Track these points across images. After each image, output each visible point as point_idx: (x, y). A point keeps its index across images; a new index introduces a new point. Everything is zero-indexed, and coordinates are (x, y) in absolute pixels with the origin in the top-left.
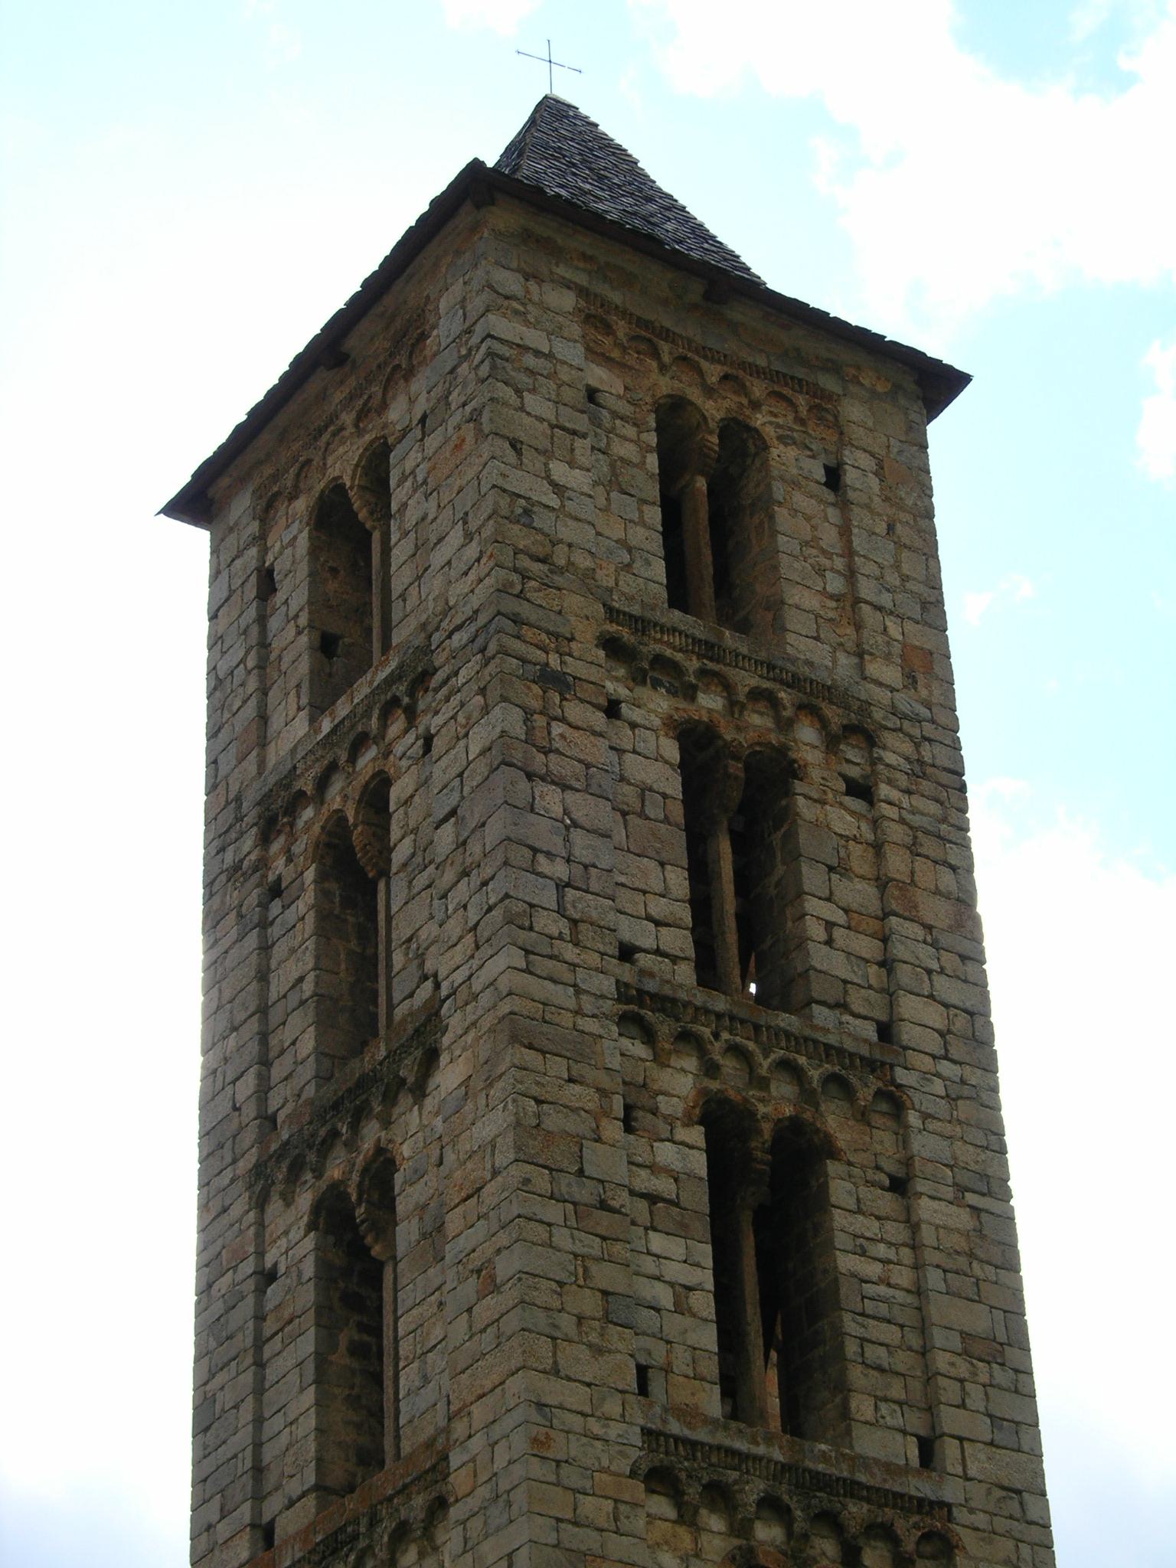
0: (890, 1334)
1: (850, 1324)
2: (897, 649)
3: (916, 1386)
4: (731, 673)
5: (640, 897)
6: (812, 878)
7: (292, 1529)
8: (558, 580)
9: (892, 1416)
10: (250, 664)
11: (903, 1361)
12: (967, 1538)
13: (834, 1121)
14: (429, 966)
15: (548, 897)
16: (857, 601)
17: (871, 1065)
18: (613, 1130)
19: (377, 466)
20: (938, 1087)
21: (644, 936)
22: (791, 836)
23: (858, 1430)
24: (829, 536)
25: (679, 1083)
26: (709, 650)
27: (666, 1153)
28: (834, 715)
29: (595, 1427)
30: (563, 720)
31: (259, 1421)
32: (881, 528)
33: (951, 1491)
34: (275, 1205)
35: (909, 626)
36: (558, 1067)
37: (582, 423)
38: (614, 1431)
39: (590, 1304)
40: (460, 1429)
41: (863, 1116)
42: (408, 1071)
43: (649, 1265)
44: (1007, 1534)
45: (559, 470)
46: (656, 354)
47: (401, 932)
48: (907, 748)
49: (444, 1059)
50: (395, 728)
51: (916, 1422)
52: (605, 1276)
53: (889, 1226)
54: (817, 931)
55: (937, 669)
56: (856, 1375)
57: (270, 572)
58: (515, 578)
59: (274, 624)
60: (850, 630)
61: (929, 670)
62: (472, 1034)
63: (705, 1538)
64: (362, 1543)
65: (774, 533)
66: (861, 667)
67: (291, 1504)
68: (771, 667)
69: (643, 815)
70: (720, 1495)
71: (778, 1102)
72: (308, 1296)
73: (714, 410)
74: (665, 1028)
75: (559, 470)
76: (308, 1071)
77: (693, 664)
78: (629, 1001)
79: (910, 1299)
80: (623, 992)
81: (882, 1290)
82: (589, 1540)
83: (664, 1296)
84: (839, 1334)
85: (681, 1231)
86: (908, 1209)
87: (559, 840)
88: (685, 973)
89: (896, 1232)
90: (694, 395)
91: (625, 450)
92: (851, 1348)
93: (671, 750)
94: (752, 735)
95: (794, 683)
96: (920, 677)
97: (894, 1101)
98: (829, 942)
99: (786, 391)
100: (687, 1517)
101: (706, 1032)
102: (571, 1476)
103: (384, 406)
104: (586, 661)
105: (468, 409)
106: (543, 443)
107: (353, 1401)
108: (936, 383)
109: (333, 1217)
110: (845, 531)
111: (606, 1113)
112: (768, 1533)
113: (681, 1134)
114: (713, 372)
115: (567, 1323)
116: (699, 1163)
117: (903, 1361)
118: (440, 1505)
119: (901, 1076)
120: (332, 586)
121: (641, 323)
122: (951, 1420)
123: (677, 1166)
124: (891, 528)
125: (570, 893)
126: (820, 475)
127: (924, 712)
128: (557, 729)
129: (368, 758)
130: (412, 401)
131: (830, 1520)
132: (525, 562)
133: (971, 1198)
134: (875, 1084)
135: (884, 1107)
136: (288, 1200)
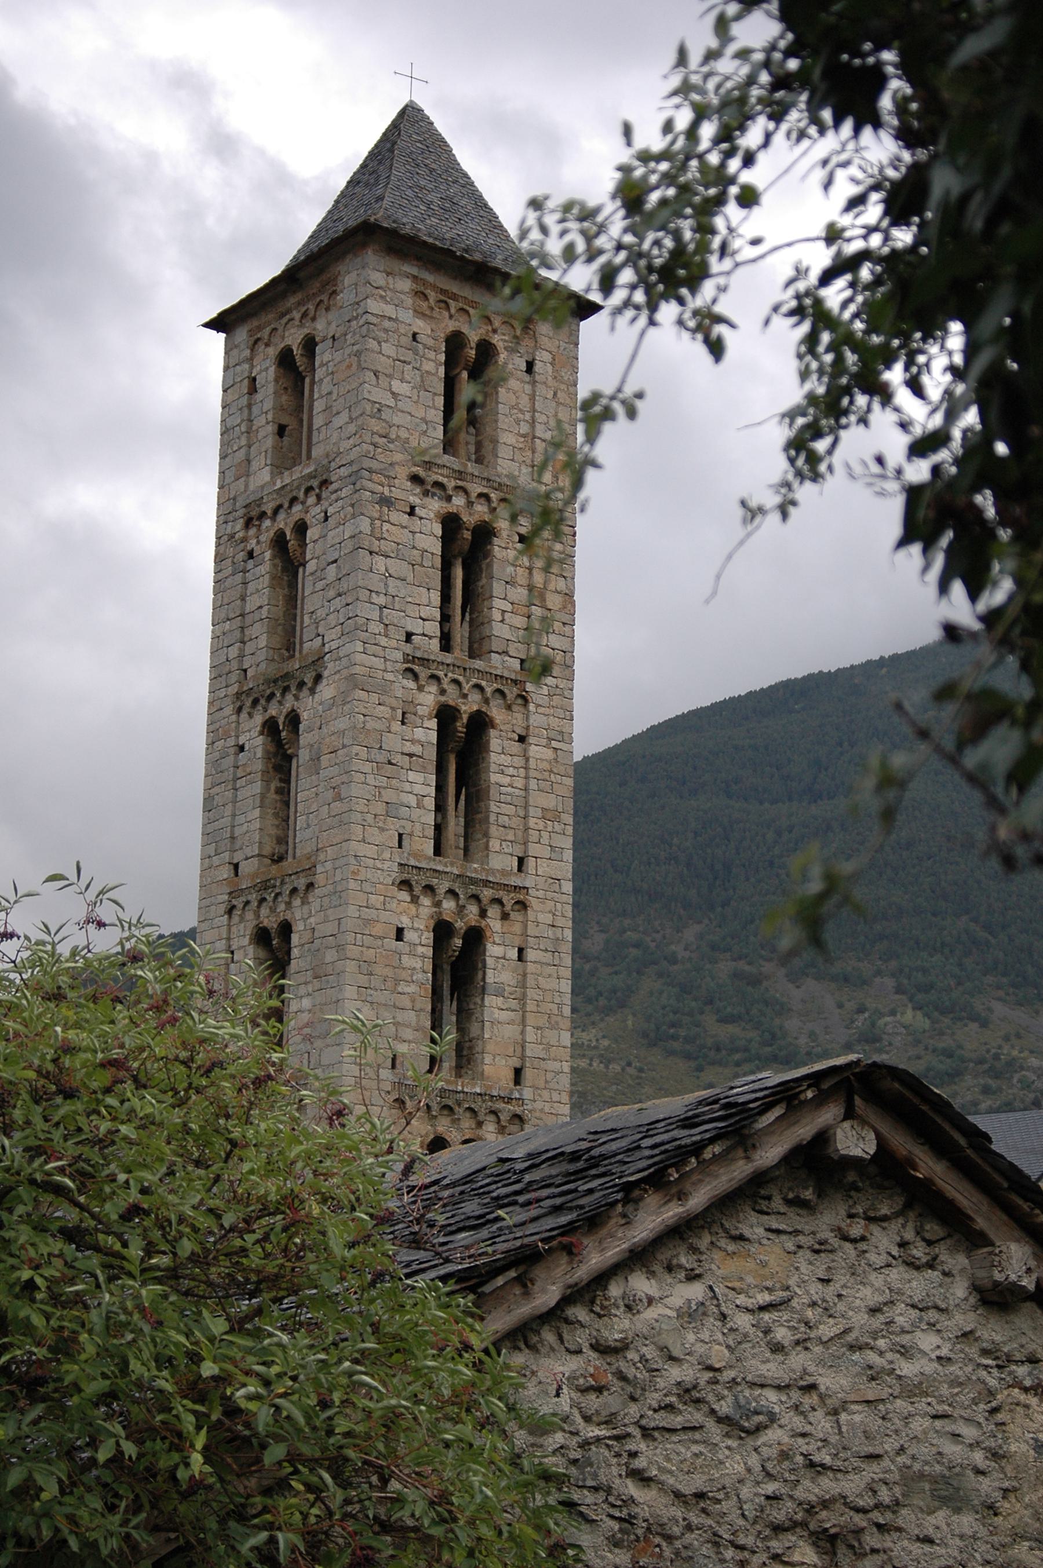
0: (510, 810)
1: (493, 807)
3: (520, 833)
4: (469, 486)
5: (417, 608)
6: (498, 588)
7: (247, 870)
10: (243, 429)
11: (516, 822)
12: (533, 902)
13: (496, 712)
14: (321, 630)
15: (376, 615)
16: (534, 437)
17: (515, 682)
18: (396, 726)
19: (310, 345)
21: (415, 626)
22: (490, 566)
23: (491, 855)
24: (525, 402)
25: (428, 700)
26: (460, 475)
27: (419, 733)
29: (379, 864)
30: (388, 522)
31: (234, 815)
32: (550, 395)
34: (244, 715)
36: (374, 698)
37: (409, 356)
38: (387, 864)
39: (380, 808)
40: (322, 857)
41: (509, 708)
42: (308, 679)
43: (407, 787)
44: (552, 900)
45: (397, 386)
46: (448, 308)
47: (309, 607)
49: (324, 682)
50: (312, 500)
51: (519, 851)
52: (389, 795)
53: (516, 759)
54: (497, 615)
56: (493, 830)
57: (254, 379)
58: (371, 448)
59: (255, 410)
60: (529, 453)
62: (337, 677)
63: (421, 908)
64: (277, 890)
65: (498, 403)
67: (247, 859)
68: (489, 480)
70: (429, 889)
71: (469, 706)
72: (259, 766)
73: (473, 337)
74: (423, 673)
75: (397, 386)
76: (262, 655)
78: (408, 662)
79: (522, 793)
80: (408, 659)
81: (509, 790)
82: (372, 914)
83: (412, 801)
84: (488, 811)
85: (423, 770)
86: (525, 750)
87: (382, 585)
88: (435, 644)
89: (519, 761)
90: (465, 329)
91: (429, 366)
92: (492, 818)
93: (438, 530)
95: (499, 487)
100: (415, 900)
101: (441, 674)
102: (367, 887)
103: (314, 319)
105: (355, 348)
106: (390, 371)
107: (276, 815)
109: (270, 727)
110: (533, 398)
111: (394, 718)
112: (449, 905)
115: (370, 818)
116: (433, 736)
117: (516, 822)
118: (310, 886)
120: (284, 398)
121: (443, 292)
122: (533, 849)
123: (423, 739)
124: (555, 394)
128: (386, 526)
129: (297, 508)
130: (329, 323)
131: (476, 898)
132: (377, 439)
133: (554, 744)
135: (520, 701)
136: (250, 715)
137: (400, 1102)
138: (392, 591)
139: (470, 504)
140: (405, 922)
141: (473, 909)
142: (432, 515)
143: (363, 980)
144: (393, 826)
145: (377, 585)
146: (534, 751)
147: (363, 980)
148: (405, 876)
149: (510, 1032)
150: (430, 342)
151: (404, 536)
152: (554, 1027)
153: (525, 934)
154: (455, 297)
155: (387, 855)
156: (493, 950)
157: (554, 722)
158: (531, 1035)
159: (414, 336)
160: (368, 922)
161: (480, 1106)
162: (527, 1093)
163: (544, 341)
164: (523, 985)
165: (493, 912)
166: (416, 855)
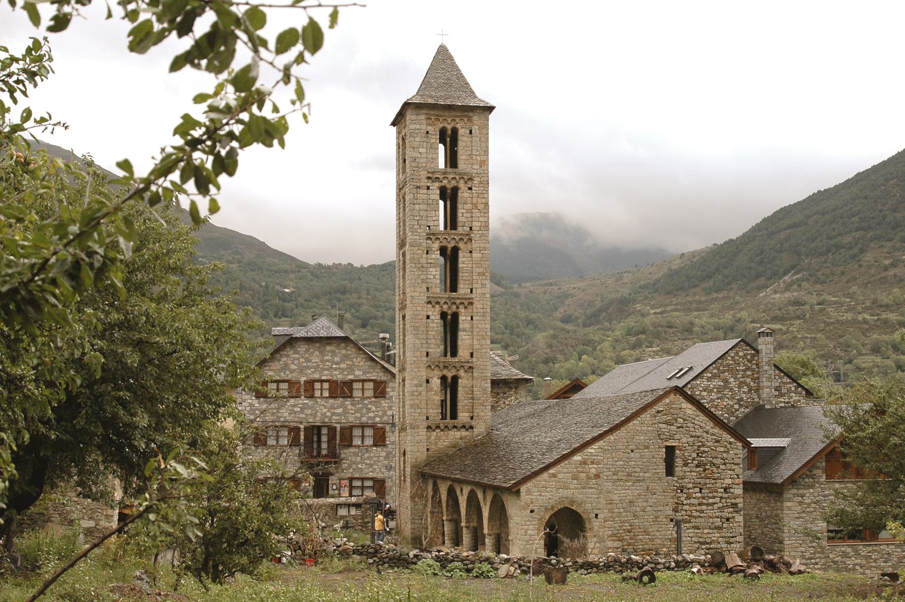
9: (466, 286)
18: (425, 256)
25: (436, 245)
27: (433, 256)
33: (473, 296)
39: (420, 281)
52: (422, 277)
70: (438, 303)
73: (449, 127)
74: (433, 238)
75: (421, 150)
77: (441, 177)
80: (427, 234)
83: (432, 277)
90: (446, 125)
93: (438, 192)
97: (470, 240)
100: (433, 307)
104: (425, 182)
108: (491, 109)
114: (449, 120)
122: (475, 286)
139: (449, 182)
140: (430, 313)
141: (454, 307)
143: (415, 332)
144: (424, 286)
146: (474, 255)
147: (415, 332)
149: (468, 342)
151: (425, 197)
152: (484, 339)
156: (461, 318)
157: (482, 245)
158: (475, 342)
159: (427, 133)
160: (417, 315)
161: (457, 365)
162: (474, 360)
164: (472, 327)
166: (433, 293)
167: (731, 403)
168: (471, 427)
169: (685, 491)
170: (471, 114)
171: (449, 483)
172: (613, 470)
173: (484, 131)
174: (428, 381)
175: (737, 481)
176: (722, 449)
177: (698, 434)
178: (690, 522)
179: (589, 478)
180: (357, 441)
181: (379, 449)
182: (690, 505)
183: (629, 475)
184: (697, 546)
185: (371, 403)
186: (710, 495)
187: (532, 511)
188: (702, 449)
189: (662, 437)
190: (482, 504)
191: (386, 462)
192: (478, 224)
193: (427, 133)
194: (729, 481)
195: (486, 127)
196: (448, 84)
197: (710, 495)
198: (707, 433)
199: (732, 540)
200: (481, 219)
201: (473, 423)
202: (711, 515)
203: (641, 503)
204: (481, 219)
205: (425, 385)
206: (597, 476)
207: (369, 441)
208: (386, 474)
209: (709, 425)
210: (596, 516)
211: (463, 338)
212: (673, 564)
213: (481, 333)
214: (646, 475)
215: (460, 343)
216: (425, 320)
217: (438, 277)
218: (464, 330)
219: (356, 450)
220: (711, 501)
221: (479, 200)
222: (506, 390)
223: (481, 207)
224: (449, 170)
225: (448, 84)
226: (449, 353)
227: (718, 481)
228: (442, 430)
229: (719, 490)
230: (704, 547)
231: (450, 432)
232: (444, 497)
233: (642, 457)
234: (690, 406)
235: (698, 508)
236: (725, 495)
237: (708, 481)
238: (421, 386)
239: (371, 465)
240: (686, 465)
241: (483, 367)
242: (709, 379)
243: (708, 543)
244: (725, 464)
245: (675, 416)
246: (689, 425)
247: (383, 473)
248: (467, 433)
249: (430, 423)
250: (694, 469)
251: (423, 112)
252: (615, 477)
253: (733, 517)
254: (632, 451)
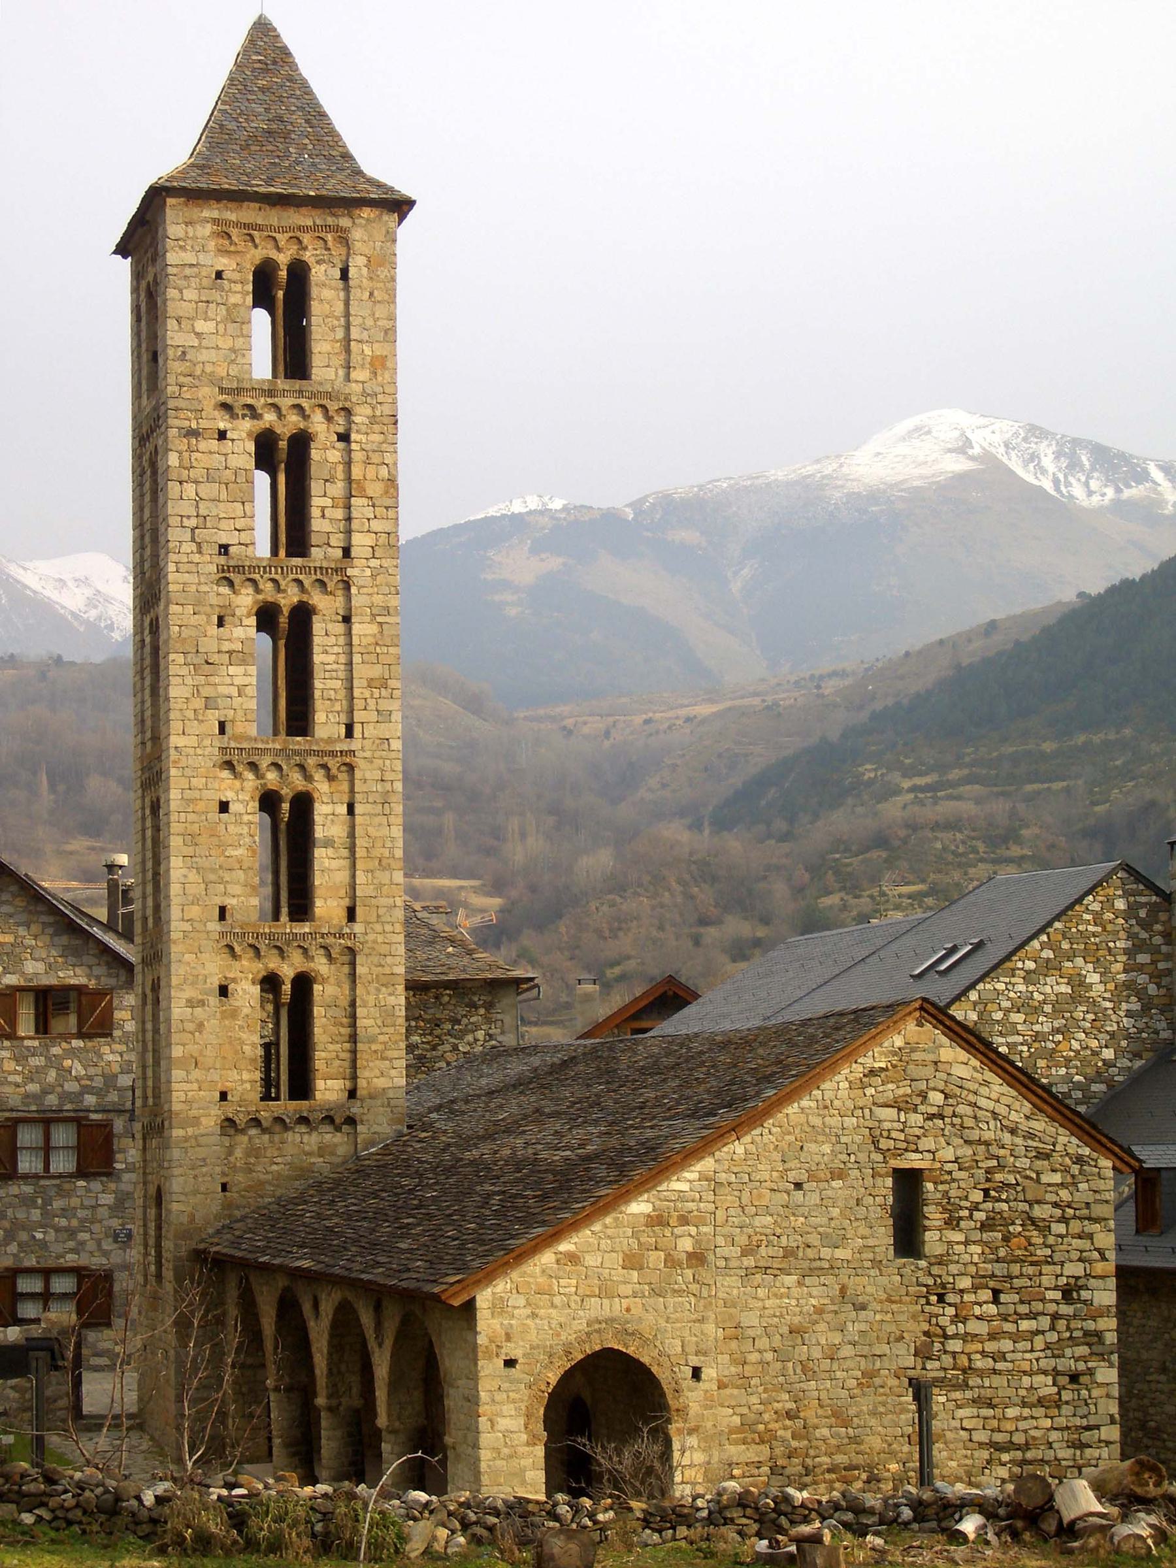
2: (369, 359)
8: (196, 382)
12: (359, 762)
13: (317, 599)
18: (213, 630)
20: (368, 572)
25: (246, 600)
28: (333, 406)
29: (199, 751)
33: (355, 745)
35: (376, 346)
39: (199, 703)
44: (381, 758)
45: (200, 326)
46: (253, 240)
48: (369, 412)
52: (206, 691)
55: (389, 364)
61: (384, 367)
63: (245, 783)
66: (348, 375)
69: (236, 482)
75: (200, 326)
77: (259, 403)
78: (223, 571)
80: (222, 569)
81: (335, 666)
82: (196, 794)
83: (234, 691)
86: (350, 629)
90: (273, 254)
91: (234, 299)
93: (251, 447)
94: (291, 426)
95: (313, 395)
96: (379, 372)
98: (323, 516)
99: (322, 235)
102: (188, 772)
108: (400, 206)
110: (347, 303)
112: (272, 776)
113: (246, 622)
119: (349, 572)
124: (371, 294)
125: (197, 531)
126: (338, 274)
127: (379, 389)
128: (195, 455)
133: (379, 619)
134: (336, 578)
137: (230, 948)
138: (202, 512)
140: (229, 796)
142: (244, 435)
143: (189, 851)
144: (213, 717)
145: (187, 508)
146: (356, 629)
147: (189, 851)
148: (227, 758)
150: (236, 276)
152: (388, 868)
153: (352, 791)
154: (259, 228)
155: (207, 742)
157: (378, 599)
158: (361, 878)
159: (219, 275)
162: (358, 928)
163: (358, 246)
164: (352, 835)
165: (319, 775)
166: (235, 738)
167: (1094, 1044)
168: (351, 1121)
169: (951, 1298)
170: (345, 222)
171: (282, 1282)
172: (742, 1240)
173: (383, 273)
174: (224, 991)
175: (1099, 1268)
176: (1057, 1178)
177: (988, 1135)
178: (966, 1386)
179: (671, 1262)
180: (27, 1163)
181: (96, 1185)
182: (966, 1337)
183: (789, 1253)
184: (985, 1454)
185: (72, 1053)
186: (1023, 1309)
187: (510, 1363)
188: (998, 1177)
189: (884, 1144)
190: (372, 1343)
191: (115, 1223)
192: (369, 540)
193: (219, 275)
194: (1076, 1269)
195: (384, 262)
196: (278, 133)
197: (1023, 1309)
198: (1013, 1132)
199: (1086, 1436)
200: (376, 525)
201: (356, 1109)
202: (1026, 1366)
203: (824, 1335)
204: (376, 525)
205: (214, 1000)
206: (697, 1258)
207: (63, 1163)
208: (116, 1258)
209: (1019, 1110)
210: (696, 1373)
211: (327, 866)
212: (907, 1513)
213: (376, 853)
214: (840, 1253)
215: (318, 879)
216: (214, 815)
217: (251, 691)
218: (329, 843)
219: (28, 1189)
220: (1025, 1325)
221: (371, 472)
222: (462, 1011)
223: (375, 489)
224: (282, 384)
225: (278, 133)
226: (284, 910)
227: (1046, 1269)
228: (265, 1131)
229: (1050, 1295)
230: (1005, 1457)
231: (289, 1136)
232: (268, 1325)
233: (823, 1203)
234: (963, 1055)
235: (990, 1347)
236: (1065, 1309)
237: (1015, 1269)
238: (202, 1003)
239: (72, 1233)
240: (952, 1223)
241: (384, 949)
242: (1029, 977)
243: (1018, 1448)
244: (1064, 1220)
245: (923, 1086)
246: (962, 1109)
247: (106, 1254)
248: (338, 1138)
249: (230, 1110)
250: (976, 1235)
251: (206, 214)
252: (749, 1262)
253: (1091, 1372)
254: (798, 1186)
